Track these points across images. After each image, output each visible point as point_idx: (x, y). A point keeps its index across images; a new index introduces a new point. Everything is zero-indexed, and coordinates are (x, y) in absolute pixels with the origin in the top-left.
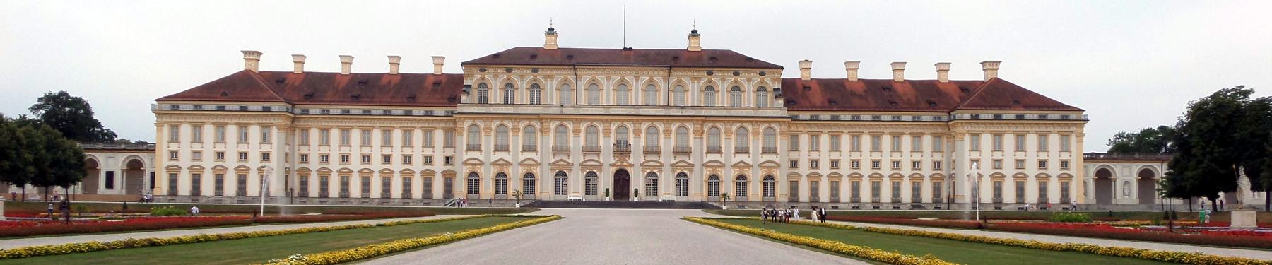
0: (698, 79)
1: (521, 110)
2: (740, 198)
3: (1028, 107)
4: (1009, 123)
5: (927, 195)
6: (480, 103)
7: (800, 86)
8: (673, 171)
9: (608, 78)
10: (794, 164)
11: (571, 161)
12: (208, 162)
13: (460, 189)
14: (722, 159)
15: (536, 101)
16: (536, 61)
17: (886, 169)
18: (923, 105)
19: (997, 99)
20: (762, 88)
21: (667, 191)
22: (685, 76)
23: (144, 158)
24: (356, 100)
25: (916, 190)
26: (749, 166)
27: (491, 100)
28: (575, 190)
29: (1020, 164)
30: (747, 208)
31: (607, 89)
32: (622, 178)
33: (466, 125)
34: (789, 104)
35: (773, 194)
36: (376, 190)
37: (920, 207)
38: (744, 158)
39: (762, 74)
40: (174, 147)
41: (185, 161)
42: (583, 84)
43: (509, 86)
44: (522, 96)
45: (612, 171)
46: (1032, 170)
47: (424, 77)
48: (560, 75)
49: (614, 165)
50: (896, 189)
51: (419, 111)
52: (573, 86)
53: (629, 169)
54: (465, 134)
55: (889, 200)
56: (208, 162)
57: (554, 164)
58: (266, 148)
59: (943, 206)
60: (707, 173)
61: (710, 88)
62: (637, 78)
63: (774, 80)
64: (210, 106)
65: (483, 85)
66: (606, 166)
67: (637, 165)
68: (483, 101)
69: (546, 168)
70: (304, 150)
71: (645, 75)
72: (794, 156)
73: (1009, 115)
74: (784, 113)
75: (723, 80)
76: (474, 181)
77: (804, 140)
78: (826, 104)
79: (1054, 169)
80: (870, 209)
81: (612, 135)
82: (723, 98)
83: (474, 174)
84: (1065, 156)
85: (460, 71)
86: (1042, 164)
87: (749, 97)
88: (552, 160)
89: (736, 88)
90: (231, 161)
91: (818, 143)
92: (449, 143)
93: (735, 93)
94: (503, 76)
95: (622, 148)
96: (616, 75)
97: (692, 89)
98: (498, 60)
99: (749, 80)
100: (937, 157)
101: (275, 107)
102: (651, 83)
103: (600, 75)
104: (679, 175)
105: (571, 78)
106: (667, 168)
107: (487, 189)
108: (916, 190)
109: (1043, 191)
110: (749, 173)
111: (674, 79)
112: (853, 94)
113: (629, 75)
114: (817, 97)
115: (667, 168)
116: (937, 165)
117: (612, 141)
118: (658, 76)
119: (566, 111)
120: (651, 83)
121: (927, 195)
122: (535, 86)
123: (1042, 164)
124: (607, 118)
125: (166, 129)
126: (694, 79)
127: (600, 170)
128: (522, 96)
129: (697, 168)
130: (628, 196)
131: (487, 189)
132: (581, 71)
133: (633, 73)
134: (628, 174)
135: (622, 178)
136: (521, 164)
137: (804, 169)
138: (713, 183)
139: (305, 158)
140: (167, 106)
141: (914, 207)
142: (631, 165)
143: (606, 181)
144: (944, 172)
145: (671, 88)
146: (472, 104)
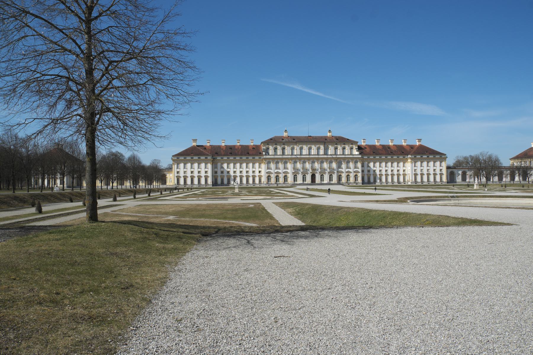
3: (430, 154)
5: (401, 180)
12: (189, 174)
13: (264, 180)
14: (343, 170)
15: (283, 153)
21: (326, 180)
24: (231, 154)
26: (351, 172)
32: (313, 177)
40: (178, 170)
41: (182, 174)
43: (275, 149)
44: (279, 152)
46: (432, 172)
51: (250, 158)
56: (189, 174)
58: (206, 170)
64: (189, 158)
65: (268, 149)
70: (216, 170)
74: (360, 156)
76: (269, 178)
79: (438, 172)
80: (385, 184)
82: (339, 152)
90: (196, 174)
100: (404, 168)
107: (273, 180)
111: (326, 146)
116: (404, 171)
125: (176, 166)
128: (279, 152)
130: (315, 182)
135: (313, 177)
139: (216, 172)
146: (266, 155)
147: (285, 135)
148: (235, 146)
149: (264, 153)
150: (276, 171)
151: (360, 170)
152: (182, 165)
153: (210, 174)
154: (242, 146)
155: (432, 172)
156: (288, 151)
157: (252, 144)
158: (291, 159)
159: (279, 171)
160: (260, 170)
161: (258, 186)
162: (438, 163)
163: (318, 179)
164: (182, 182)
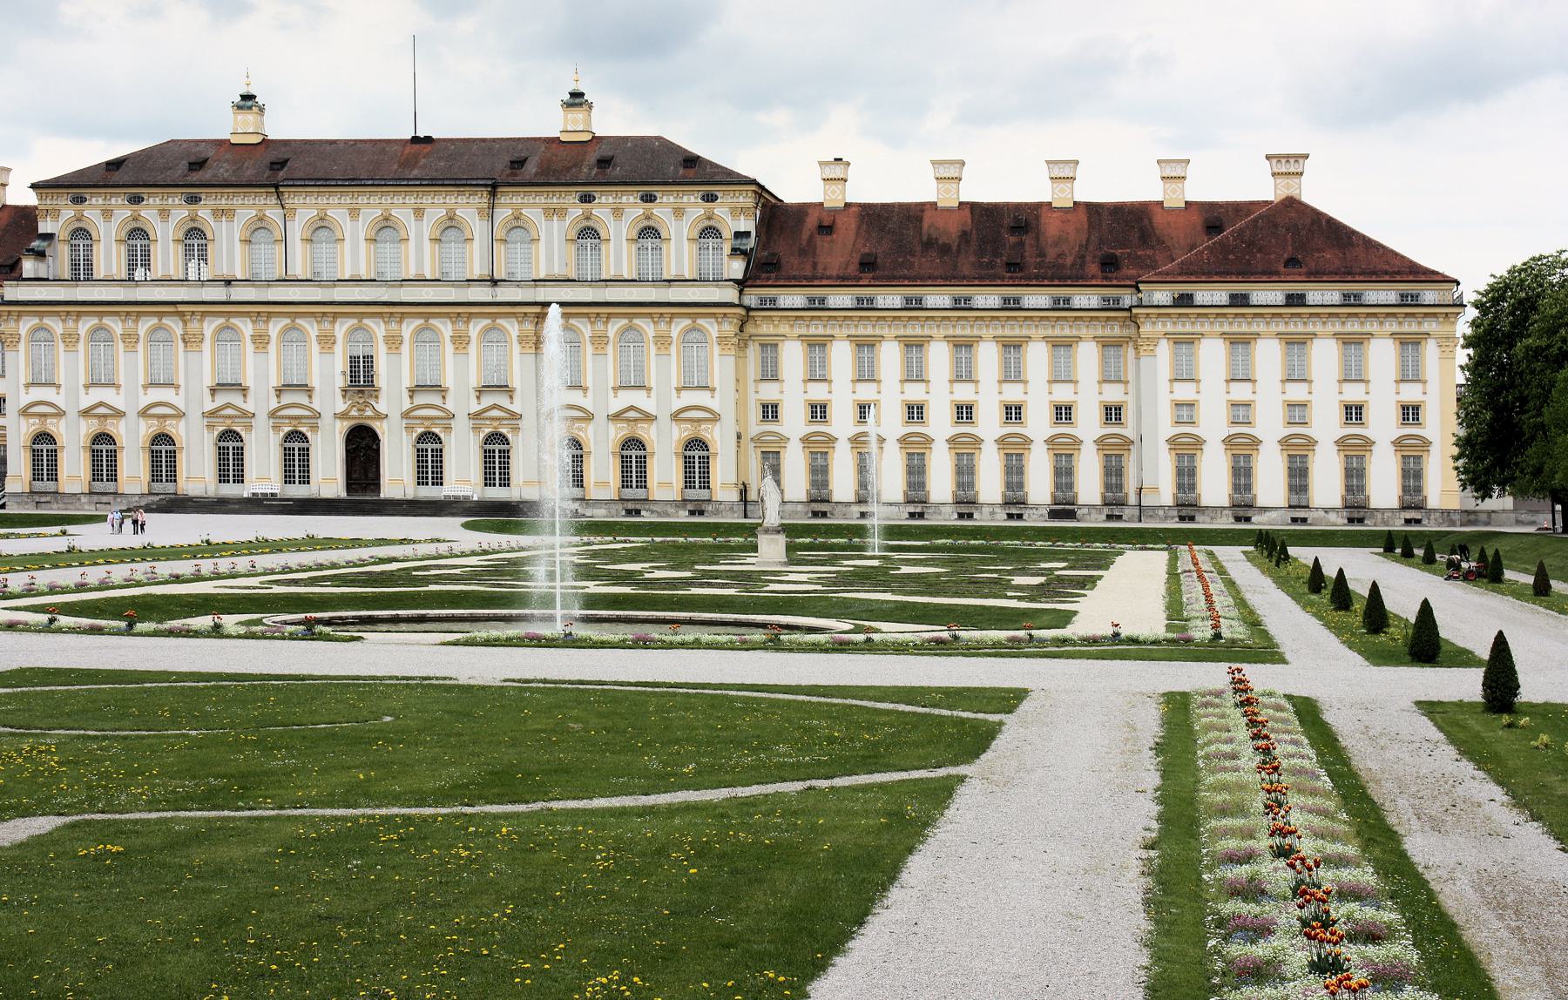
0: (561, 212)
2: (629, 493)
4: (1268, 313)
5: (1089, 487)
6: (75, 279)
7: (811, 222)
8: (476, 429)
9: (354, 213)
10: (770, 411)
11: (249, 407)
16: (205, 175)
17: (989, 424)
18: (1093, 268)
19: (1283, 251)
22: (530, 206)
25: (1064, 474)
26: (649, 418)
27: (100, 272)
28: (263, 472)
29: (1297, 411)
30: (646, 517)
31: (348, 239)
33: (26, 326)
35: (706, 484)
37: (1071, 515)
39: (710, 198)
42: (297, 229)
45: (342, 428)
46: (1326, 426)
48: (248, 207)
49: (343, 416)
50: (1014, 471)
52: (278, 235)
53: (377, 426)
54: (22, 346)
55: (850, 497)
57: (213, 414)
59: (1127, 512)
62: (419, 212)
63: (736, 212)
65: (81, 233)
66: (326, 421)
67: (395, 416)
68: (82, 271)
69: (195, 420)
71: (437, 205)
72: (769, 392)
73: (1322, 294)
75: (616, 214)
77: (792, 356)
78: (853, 269)
79: (1383, 426)
81: (339, 348)
83: (43, 437)
84: (1411, 393)
86: (1354, 412)
88: (209, 406)
89: (649, 232)
91: (824, 363)
93: (649, 243)
94: (123, 212)
95: (361, 376)
96: (373, 205)
97: (543, 237)
98: (116, 177)
99: (679, 212)
100: (1113, 394)
102: (451, 223)
103: (336, 206)
104: (490, 439)
105: (274, 214)
106: (461, 425)
108: (1064, 474)
109: (1355, 476)
110: (648, 433)
111: (503, 213)
112: (929, 244)
113: (401, 206)
114: (839, 252)
115: (461, 425)
116: (1113, 413)
117: (340, 364)
118: (468, 207)
119: (239, 293)
120: (451, 223)
121: (1089, 487)
123: (1354, 412)
124: (328, 310)
126: (550, 212)
127: (314, 428)
130: (375, 484)
131: (74, 470)
132: (294, 199)
133: (410, 200)
134: (375, 437)
135: (362, 448)
136: (144, 413)
137: (794, 422)
141: (1054, 514)
142: (381, 417)
144: (1128, 431)
145: (497, 235)
150: (86, 401)
156: (230, 250)
159: (107, 395)
163: (397, 474)
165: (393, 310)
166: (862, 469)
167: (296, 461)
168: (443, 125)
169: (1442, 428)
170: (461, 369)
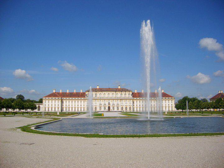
1: (95, 98)
3: (167, 97)
20: (129, 94)
21: (116, 110)
22: (118, 92)
23: (41, 106)
32: (109, 108)
34: (133, 97)
36: (73, 110)
38: (127, 104)
41: (47, 106)
44: (94, 96)
46: (167, 106)
47: (79, 93)
48: (100, 92)
51: (80, 98)
60: (121, 107)
61: (121, 94)
64: (51, 98)
71: (112, 92)
74: (132, 98)
75: (123, 93)
79: (170, 105)
85: (84, 92)
87: (127, 96)
89: (125, 94)
92: (84, 103)
95: (109, 104)
97: (119, 94)
101: (60, 98)
110: (127, 107)
118: (114, 93)
122: (96, 94)
123: (169, 105)
124: (108, 99)
128: (94, 96)
129: (120, 106)
135: (109, 108)
138: (122, 108)
140: (44, 98)
143: (107, 108)
147: (98, 87)
148: (73, 93)
149: (86, 96)
151: (132, 105)
152: (47, 101)
153: (60, 106)
154: (77, 93)
155: (167, 106)
157: (81, 92)
158: (99, 99)
160: (84, 104)
161: (83, 112)
162: (170, 101)
164: (47, 110)
165: (112, 99)
166: (133, 109)
167: (105, 108)
168: (110, 87)
169: (174, 106)
170: (115, 102)
